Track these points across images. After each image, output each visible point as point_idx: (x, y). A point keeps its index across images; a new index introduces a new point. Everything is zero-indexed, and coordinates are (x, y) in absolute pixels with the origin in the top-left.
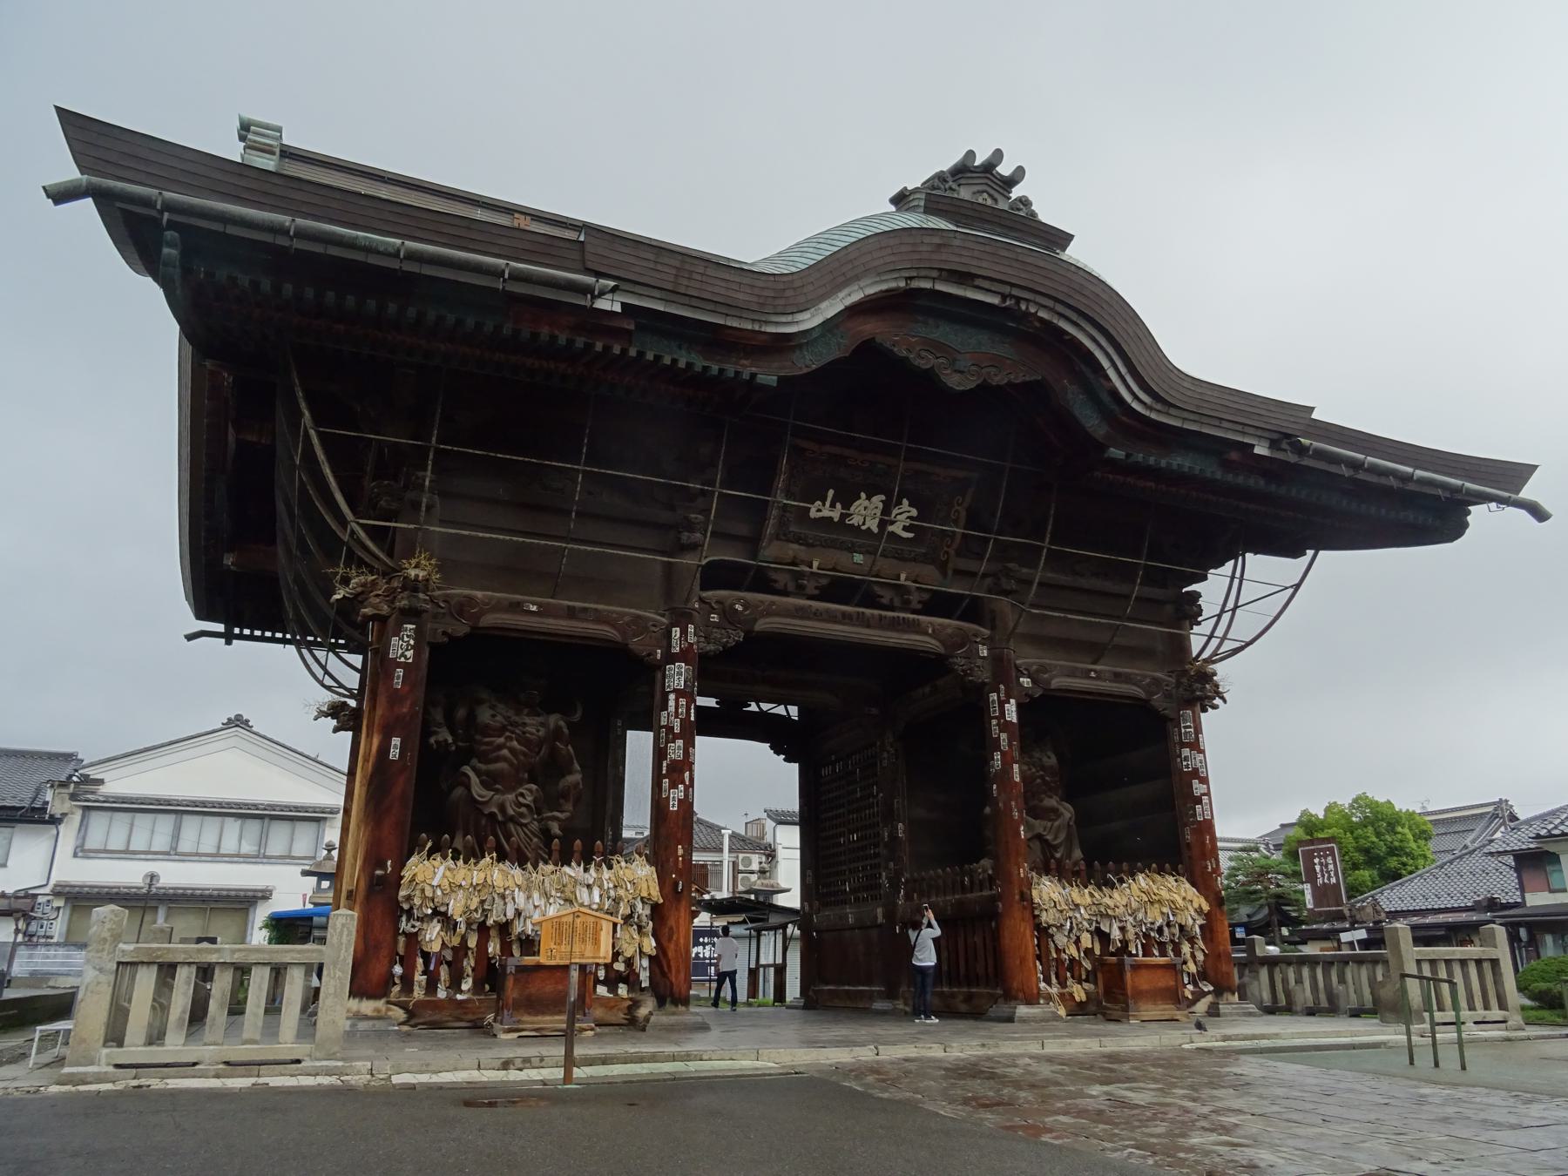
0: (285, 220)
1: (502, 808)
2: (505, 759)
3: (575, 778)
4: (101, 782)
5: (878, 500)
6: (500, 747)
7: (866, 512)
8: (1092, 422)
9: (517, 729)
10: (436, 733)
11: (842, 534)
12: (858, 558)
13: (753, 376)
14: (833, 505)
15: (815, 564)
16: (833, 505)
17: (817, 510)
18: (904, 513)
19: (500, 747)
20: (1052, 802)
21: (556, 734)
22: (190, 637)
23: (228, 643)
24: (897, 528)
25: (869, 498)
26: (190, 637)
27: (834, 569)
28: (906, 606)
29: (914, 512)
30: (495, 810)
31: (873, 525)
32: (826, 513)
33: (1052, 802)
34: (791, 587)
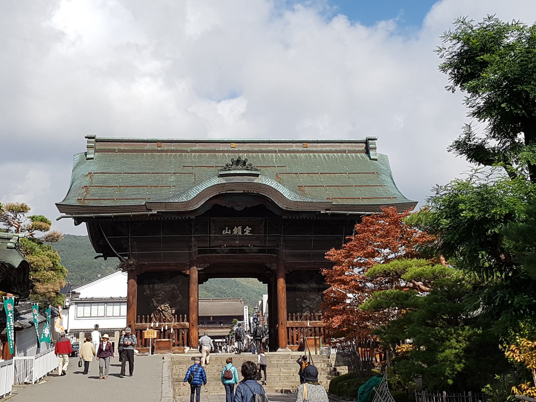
0: (92, 215)
1: (161, 308)
2: (160, 296)
3: (178, 299)
4: (79, 294)
5: (240, 228)
6: (160, 293)
7: (237, 231)
8: (276, 212)
9: (163, 288)
10: (145, 291)
11: (233, 237)
12: (237, 242)
13: (189, 218)
14: (228, 231)
15: (225, 246)
16: (228, 231)
17: (225, 232)
18: (248, 230)
19: (160, 293)
20: (312, 296)
21: (174, 289)
22: (96, 258)
23: (106, 259)
24: (247, 233)
25: (237, 227)
26: (96, 258)
27: (231, 246)
28: (252, 252)
29: (250, 229)
30: (159, 308)
31: (240, 233)
32: (227, 232)
33: (312, 296)
34: (220, 251)
